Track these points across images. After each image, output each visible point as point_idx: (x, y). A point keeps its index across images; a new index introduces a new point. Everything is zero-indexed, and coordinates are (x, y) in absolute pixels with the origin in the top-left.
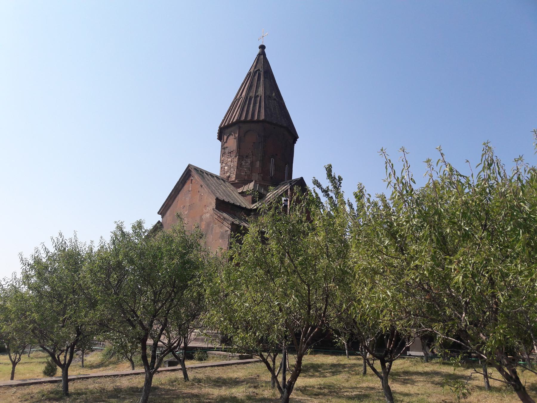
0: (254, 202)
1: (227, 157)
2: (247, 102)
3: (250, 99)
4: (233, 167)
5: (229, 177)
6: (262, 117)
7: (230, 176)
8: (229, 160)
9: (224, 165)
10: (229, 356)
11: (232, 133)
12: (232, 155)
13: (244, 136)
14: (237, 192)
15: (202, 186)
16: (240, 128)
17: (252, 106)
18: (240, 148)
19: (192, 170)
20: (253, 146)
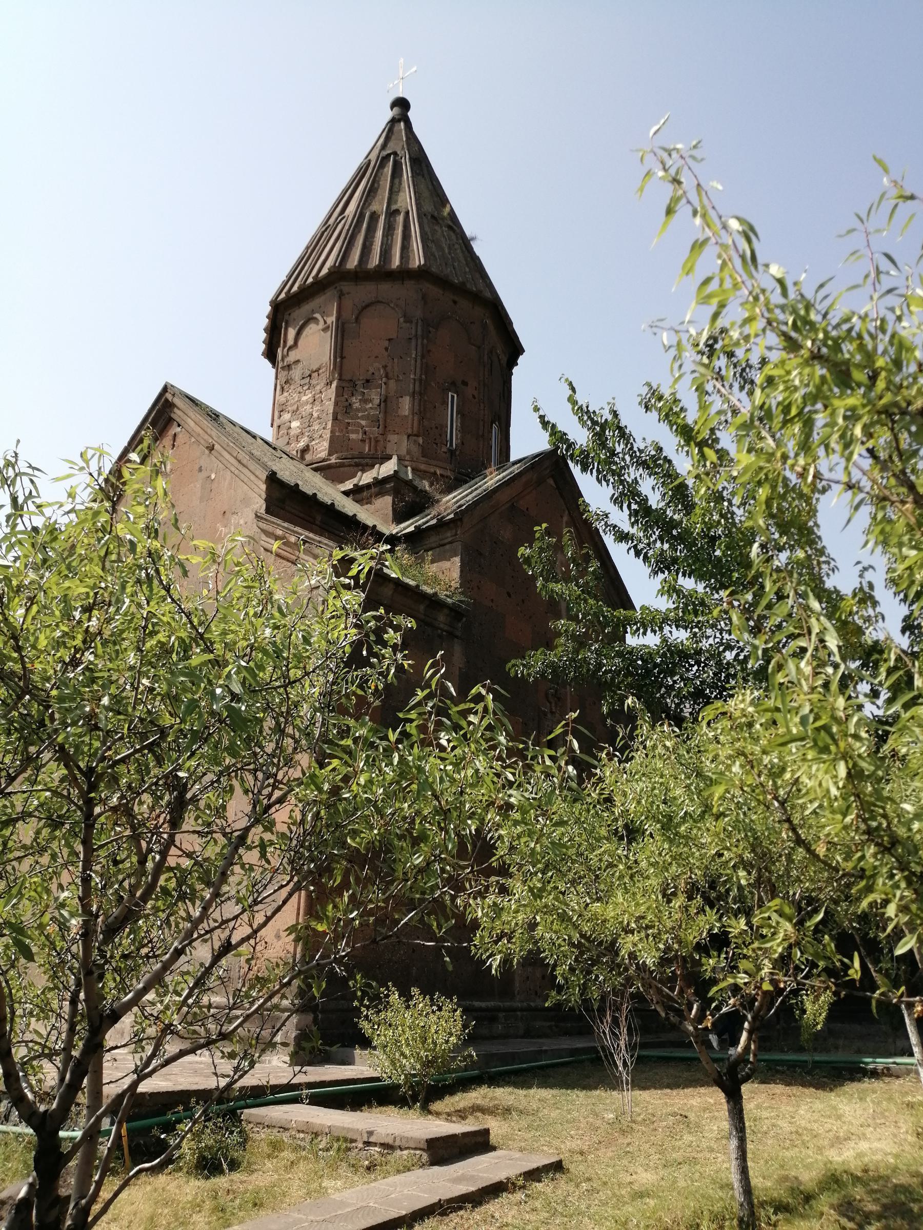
0: (399, 518)
1: (300, 389)
2: (365, 225)
3: (374, 217)
4: (319, 418)
5: (305, 450)
6: (418, 259)
7: (308, 446)
8: (304, 398)
9: (286, 416)
10: (368, 1143)
11: (317, 316)
12: (314, 382)
13: (357, 319)
14: (337, 490)
15: (211, 448)
16: (341, 295)
17: (379, 233)
18: (342, 358)
19: (177, 401)
20: (386, 349)
